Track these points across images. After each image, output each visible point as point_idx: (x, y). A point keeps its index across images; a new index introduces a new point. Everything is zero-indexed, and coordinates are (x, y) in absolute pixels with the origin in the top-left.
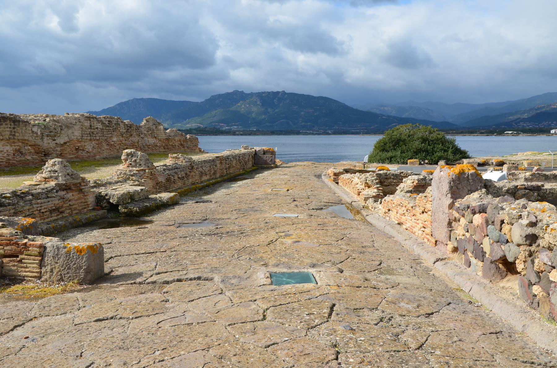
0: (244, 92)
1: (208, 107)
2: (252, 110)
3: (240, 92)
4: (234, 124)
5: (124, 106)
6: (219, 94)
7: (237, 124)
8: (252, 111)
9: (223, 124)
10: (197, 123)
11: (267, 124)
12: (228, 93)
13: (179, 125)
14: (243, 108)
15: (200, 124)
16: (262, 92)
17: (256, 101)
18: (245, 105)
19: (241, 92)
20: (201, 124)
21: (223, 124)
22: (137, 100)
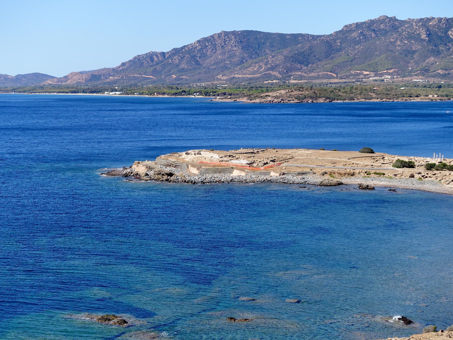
0: (397, 18)
1: (339, 44)
2: (414, 49)
3: (389, 18)
4: (385, 71)
5: (207, 44)
6: (357, 23)
7: (391, 71)
8: (414, 51)
9: (367, 73)
10: (327, 71)
11: (440, 71)
12: (371, 20)
13: (297, 73)
14: (399, 46)
15: (331, 72)
16: (428, 19)
17: (419, 34)
18: (401, 41)
19: (391, 18)
20: (333, 73)
21: (367, 73)
22: (226, 34)
